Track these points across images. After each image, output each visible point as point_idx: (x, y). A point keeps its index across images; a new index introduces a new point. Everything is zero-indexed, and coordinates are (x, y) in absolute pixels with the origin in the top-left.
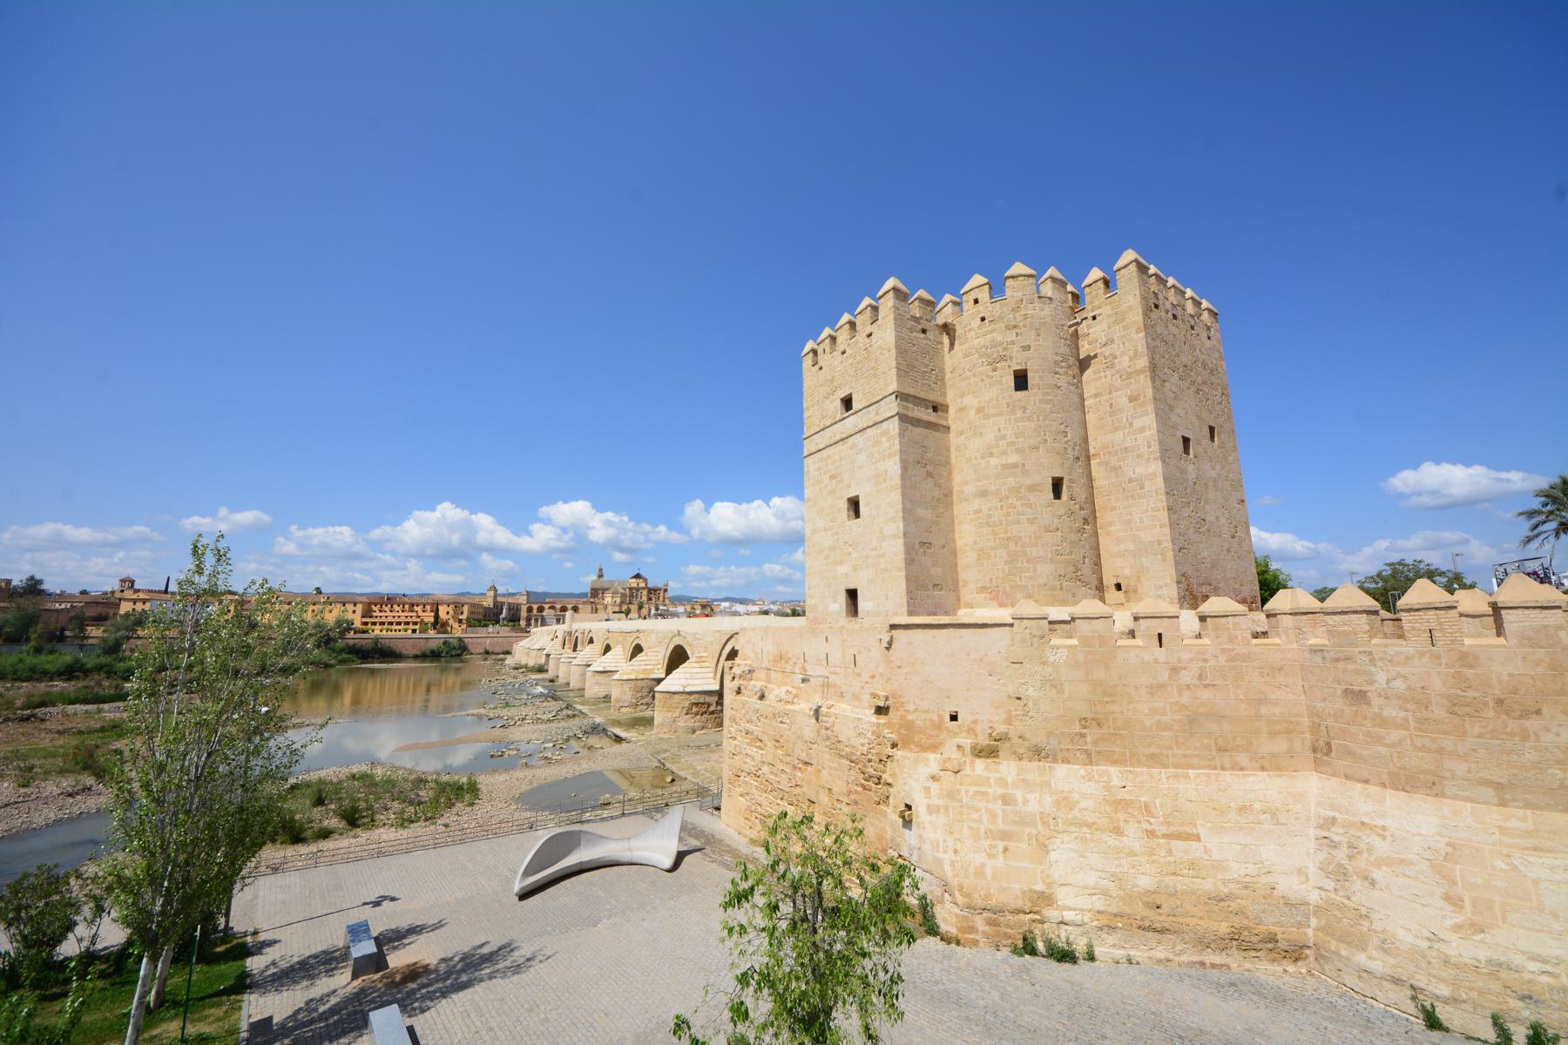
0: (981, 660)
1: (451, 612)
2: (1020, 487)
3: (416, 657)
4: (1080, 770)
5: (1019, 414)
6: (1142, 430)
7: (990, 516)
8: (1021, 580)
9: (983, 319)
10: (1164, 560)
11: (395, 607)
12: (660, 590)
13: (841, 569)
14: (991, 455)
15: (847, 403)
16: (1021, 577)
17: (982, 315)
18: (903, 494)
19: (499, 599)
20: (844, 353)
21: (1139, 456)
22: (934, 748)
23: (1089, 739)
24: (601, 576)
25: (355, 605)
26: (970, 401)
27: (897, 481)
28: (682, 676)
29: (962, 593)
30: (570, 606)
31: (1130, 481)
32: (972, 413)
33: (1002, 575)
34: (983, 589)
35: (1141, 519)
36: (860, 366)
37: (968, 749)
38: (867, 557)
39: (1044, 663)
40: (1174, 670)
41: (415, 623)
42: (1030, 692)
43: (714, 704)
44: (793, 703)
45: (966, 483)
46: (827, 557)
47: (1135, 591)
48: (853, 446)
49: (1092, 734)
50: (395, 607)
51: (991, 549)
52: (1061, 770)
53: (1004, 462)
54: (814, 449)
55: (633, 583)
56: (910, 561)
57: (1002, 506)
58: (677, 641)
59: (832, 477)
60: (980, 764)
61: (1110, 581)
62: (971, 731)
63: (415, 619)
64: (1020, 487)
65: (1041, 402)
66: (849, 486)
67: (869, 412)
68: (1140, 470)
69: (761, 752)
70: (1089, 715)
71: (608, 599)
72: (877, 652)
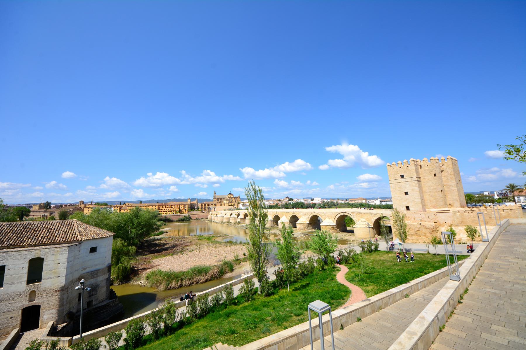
1: (183, 207)
3: (177, 221)
6: (453, 183)
9: (427, 165)
10: (458, 201)
11: (167, 206)
12: (238, 198)
13: (403, 203)
19: (191, 203)
21: (453, 186)
22: (444, 226)
24: (215, 194)
25: (155, 206)
30: (214, 204)
31: (451, 190)
32: (427, 180)
37: (448, 226)
40: (471, 216)
41: (174, 211)
42: (455, 219)
45: (426, 190)
47: (453, 206)
49: (462, 223)
50: (167, 206)
58: (314, 214)
59: (399, 188)
62: (448, 224)
63: (173, 210)
66: (405, 190)
71: (225, 201)
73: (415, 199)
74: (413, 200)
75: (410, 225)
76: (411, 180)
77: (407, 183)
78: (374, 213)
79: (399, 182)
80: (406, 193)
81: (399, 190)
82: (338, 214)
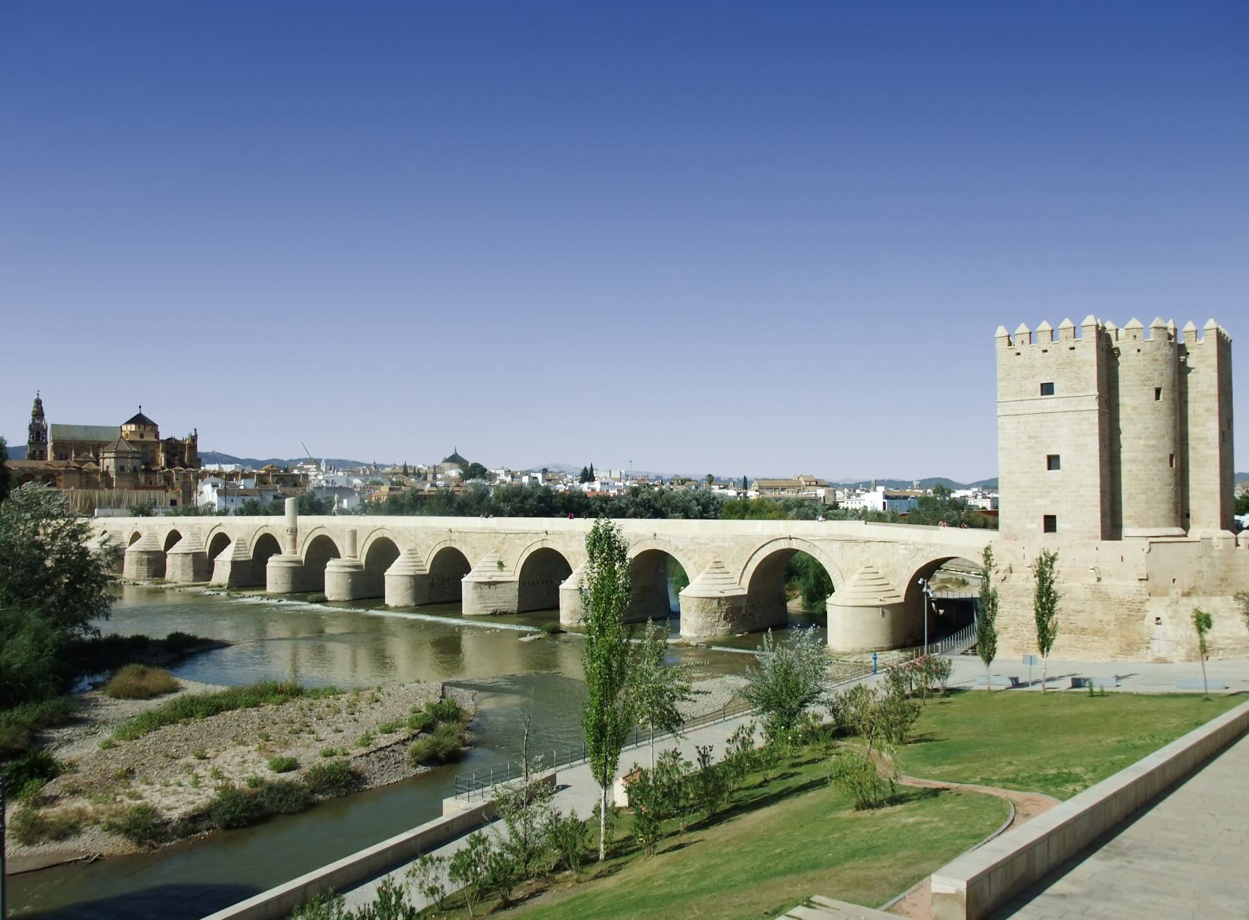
4: (1218, 598)
5: (1157, 415)
7: (1137, 475)
9: (1139, 351)
13: (1039, 502)
14: (1140, 438)
20: (1045, 351)
21: (1208, 444)
22: (1166, 595)
24: (39, 413)
36: (1062, 366)
39: (1210, 557)
52: (1213, 599)
59: (1030, 437)
66: (1050, 447)
67: (1071, 402)
72: (1142, 555)
76: (1078, 408)
78: (914, 544)
79: (1032, 411)
80: (1053, 462)
82: (763, 546)
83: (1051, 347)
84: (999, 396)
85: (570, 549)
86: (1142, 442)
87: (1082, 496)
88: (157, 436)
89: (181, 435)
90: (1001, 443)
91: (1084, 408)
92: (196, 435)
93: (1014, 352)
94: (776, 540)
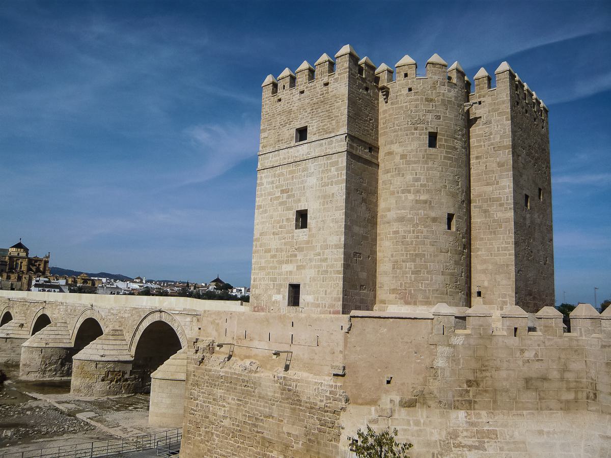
0: (411, 342)
2: (427, 218)
8: (422, 286)
9: (410, 90)
12: (41, 261)
13: (287, 268)
14: (409, 192)
15: (302, 134)
16: (422, 283)
17: (410, 86)
18: (346, 214)
20: (302, 92)
21: (501, 205)
22: (374, 402)
23: (471, 394)
26: (396, 148)
27: (342, 204)
28: (99, 346)
29: (379, 292)
33: (409, 281)
34: (393, 291)
35: (498, 248)
36: (316, 106)
38: (310, 260)
43: (129, 373)
44: (256, 372)
45: (389, 210)
46: (274, 256)
48: (305, 170)
49: (472, 390)
51: (403, 261)
53: (418, 198)
54: (268, 165)
55: (13, 251)
56: (347, 266)
57: (414, 231)
58: (88, 315)
60: (404, 411)
61: (474, 289)
64: (427, 218)
65: (445, 158)
66: (299, 200)
67: (321, 145)
68: (500, 215)
69: (223, 409)
70: (472, 378)
72: (339, 336)
73: (327, 247)
74: (318, 250)
75: (243, 381)
77: (311, 166)
81: (281, 204)
82: (145, 318)
83: (307, 87)
84: (261, 149)
85: (54, 315)
86: (411, 197)
87: (325, 260)
88: (27, 254)
89: (41, 256)
90: (259, 201)
91: (334, 151)
92: (49, 256)
93: (276, 99)
94: (153, 312)
